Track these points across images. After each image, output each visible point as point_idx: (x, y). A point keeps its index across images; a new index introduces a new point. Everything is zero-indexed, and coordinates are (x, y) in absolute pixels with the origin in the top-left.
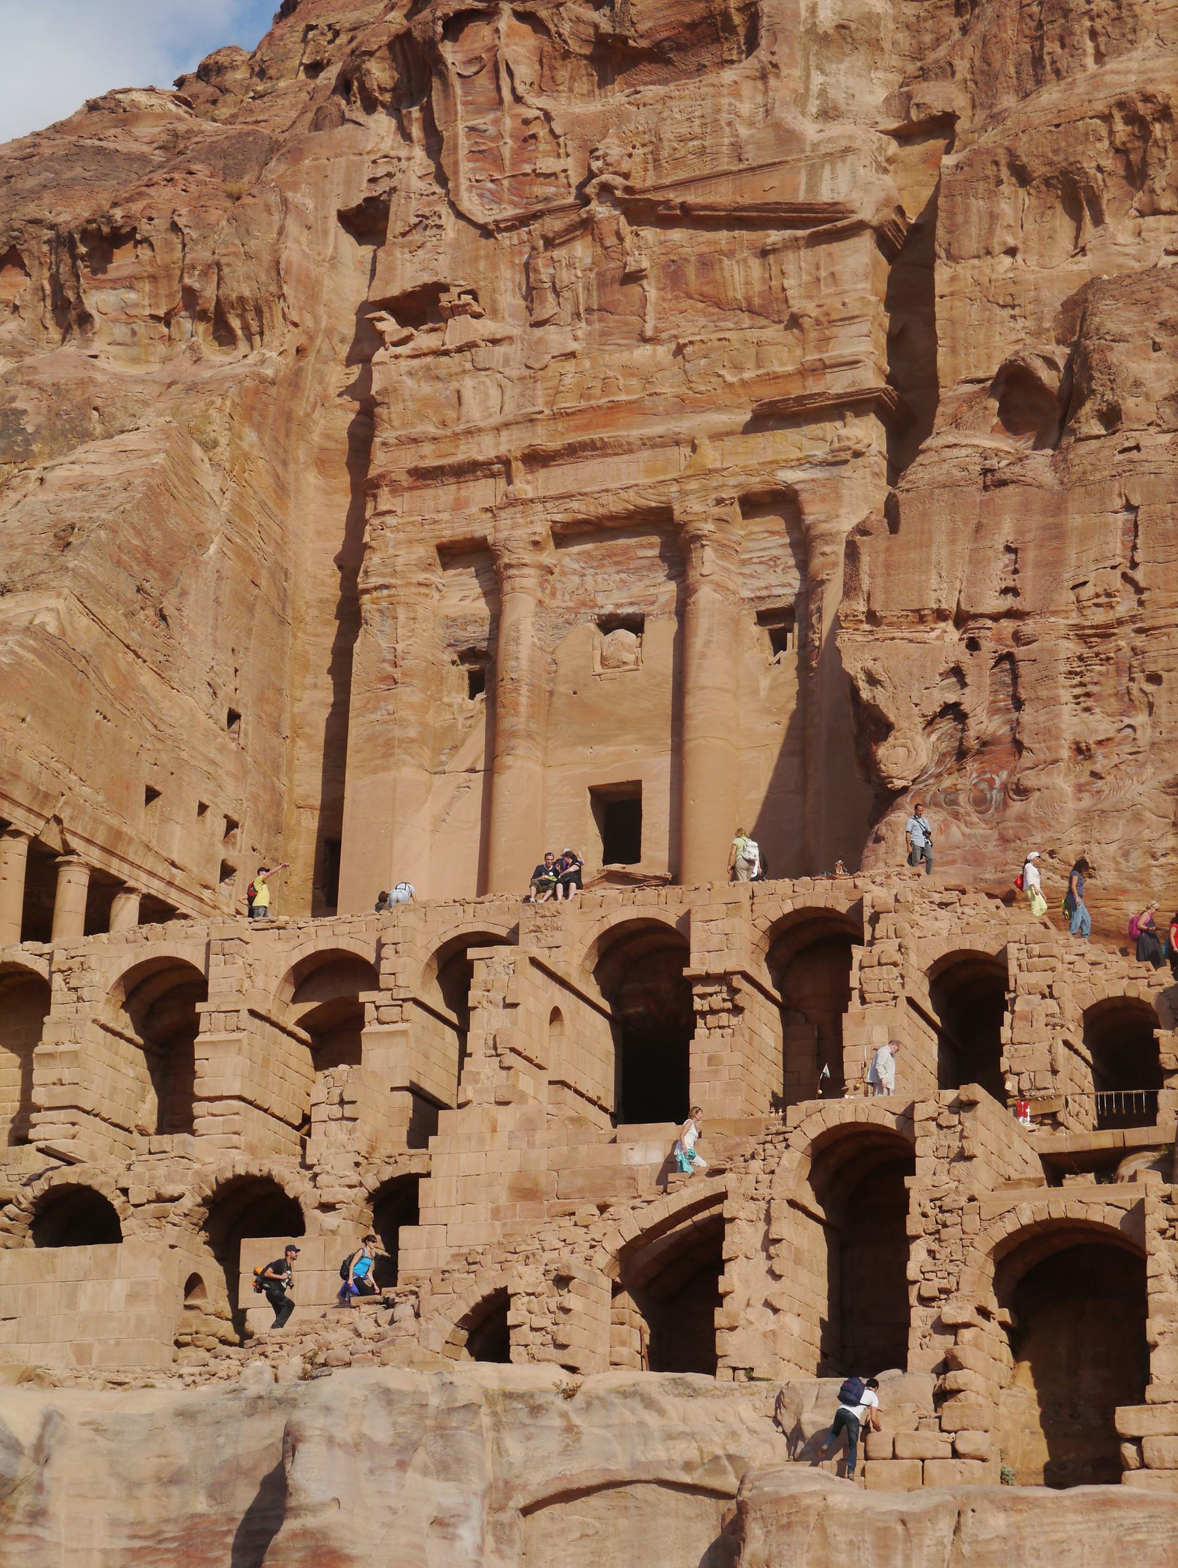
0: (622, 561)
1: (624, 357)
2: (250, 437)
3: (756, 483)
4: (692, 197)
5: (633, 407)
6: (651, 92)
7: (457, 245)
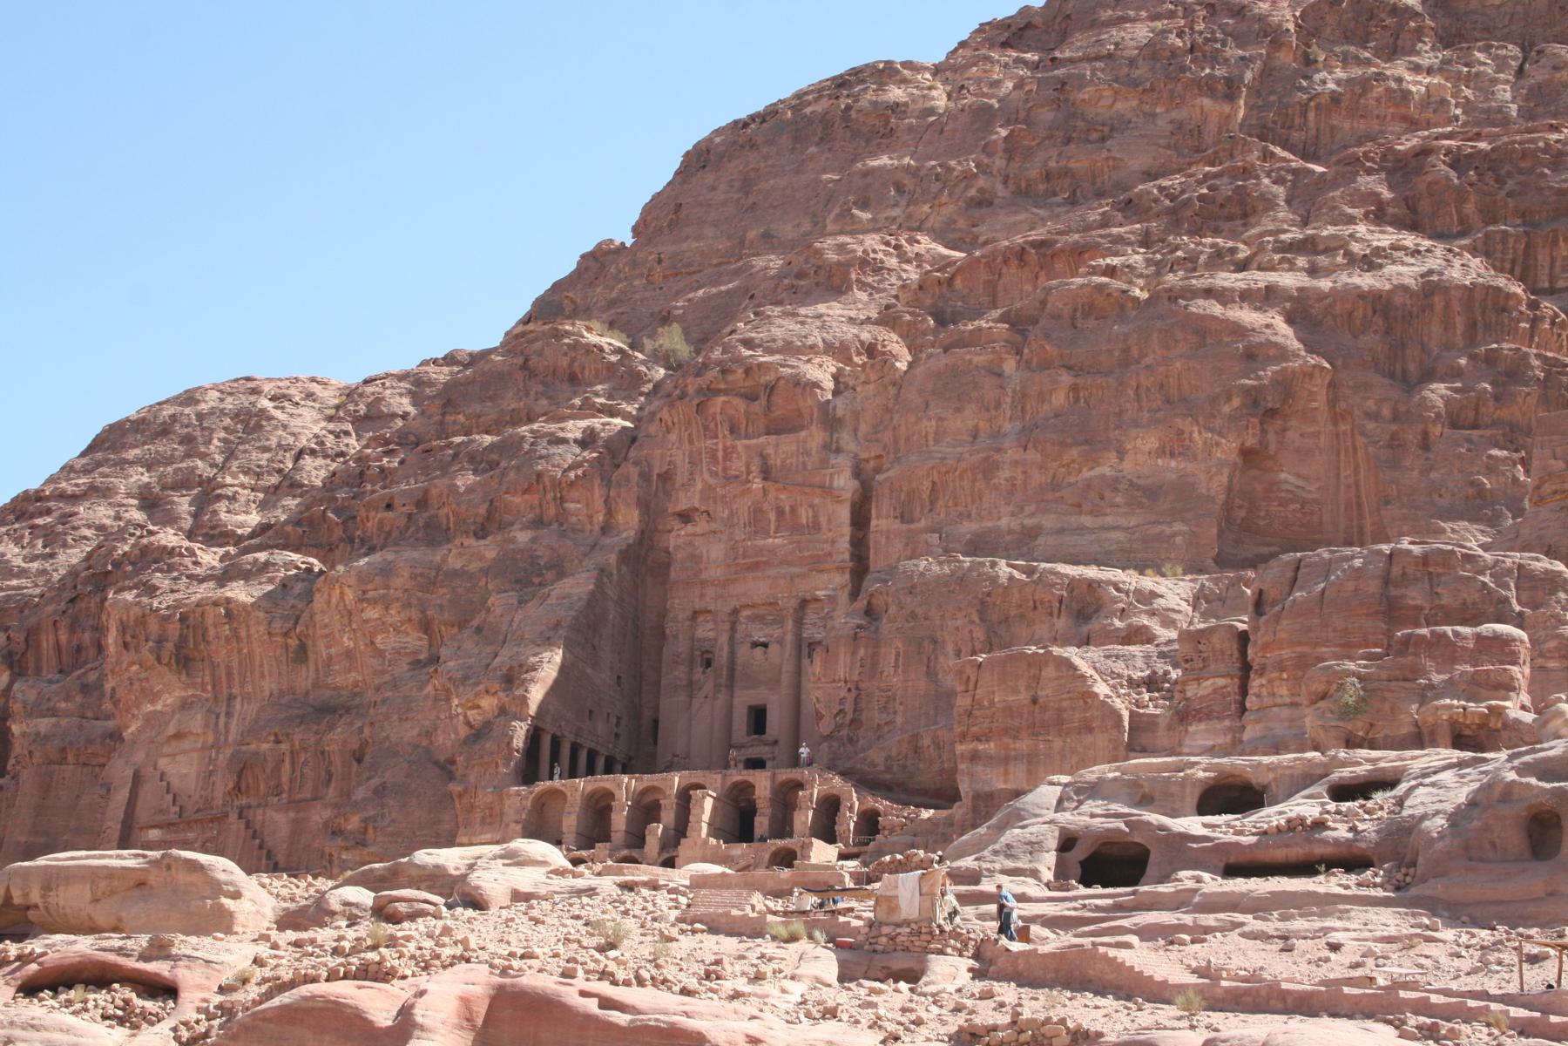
1: (760, 543)
2: (624, 569)
5: (766, 563)
7: (701, 492)
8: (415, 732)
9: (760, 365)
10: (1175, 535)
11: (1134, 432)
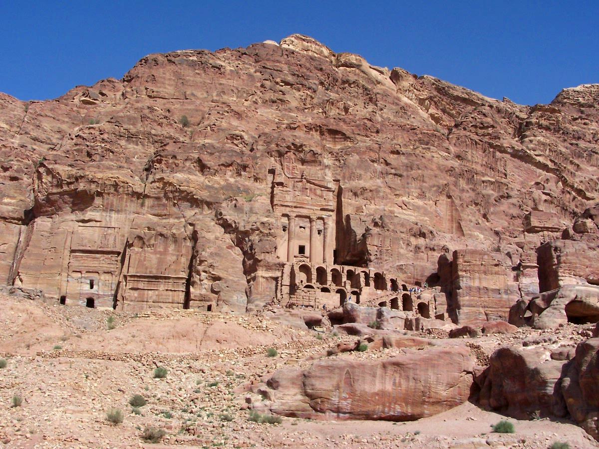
0: (303, 221)
3: (320, 216)
4: (313, 181)
6: (309, 167)
8: (214, 236)
9: (304, 145)
10: (426, 220)
11: (412, 190)
